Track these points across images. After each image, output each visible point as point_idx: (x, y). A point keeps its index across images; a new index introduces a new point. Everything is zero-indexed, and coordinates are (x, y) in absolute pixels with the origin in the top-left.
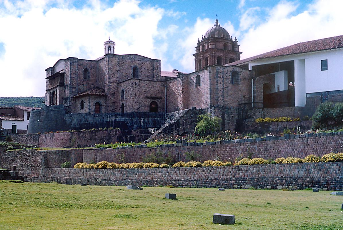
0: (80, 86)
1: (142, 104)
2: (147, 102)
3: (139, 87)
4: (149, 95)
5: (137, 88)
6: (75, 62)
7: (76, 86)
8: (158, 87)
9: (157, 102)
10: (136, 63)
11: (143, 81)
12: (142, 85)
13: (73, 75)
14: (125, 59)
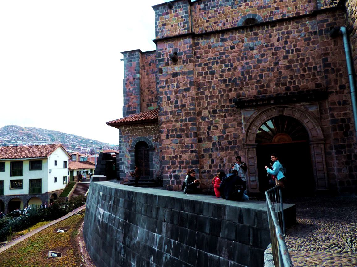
0: (151, 105)
1: (215, 139)
2: (240, 124)
3: (190, 66)
4: (250, 91)
5: (184, 73)
6: (132, 60)
7: (135, 108)
8: (301, 45)
9: (297, 115)
10: (251, 7)
11: (213, 40)
12: (210, 55)
13: (130, 87)
14: (213, 7)
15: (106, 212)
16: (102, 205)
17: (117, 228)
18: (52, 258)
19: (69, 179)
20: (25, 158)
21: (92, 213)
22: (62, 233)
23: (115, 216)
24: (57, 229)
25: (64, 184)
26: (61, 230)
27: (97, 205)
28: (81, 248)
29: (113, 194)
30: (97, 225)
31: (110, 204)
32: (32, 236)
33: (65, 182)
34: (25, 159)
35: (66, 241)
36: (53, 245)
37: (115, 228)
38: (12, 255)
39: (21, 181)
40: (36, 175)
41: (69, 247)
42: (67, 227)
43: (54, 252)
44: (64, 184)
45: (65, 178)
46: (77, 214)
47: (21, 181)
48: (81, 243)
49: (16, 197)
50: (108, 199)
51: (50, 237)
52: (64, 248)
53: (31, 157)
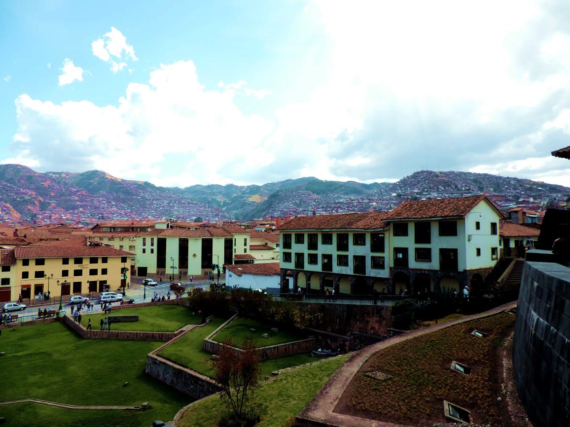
15: (541, 320)
16: (535, 306)
17: (558, 355)
18: (454, 372)
19: (501, 252)
20: (433, 217)
21: (522, 317)
22: (478, 338)
23: (555, 330)
24: (471, 330)
25: (492, 259)
26: (477, 333)
27: (529, 304)
28: (505, 371)
29: (554, 289)
30: (528, 339)
31: (548, 306)
32: (434, 332)
33: (494, 256)
34: (433, 219)
35: (481, 351)
36: (460, 353)
37: (556, 353)
38: (405, 351)
39: (429, 250)
40: (448, 242)
41: (484, 364)
42: (487, 331)
43: (460, 364)
44: (492, 259)
45: (494, 250)
46: (508, 312)
47: (429, 250)
48: (506, 363)
49: (423, 272)
50: (545, 297)
51: (459, 340)
52: (476, 362)
53: (440, 217)
